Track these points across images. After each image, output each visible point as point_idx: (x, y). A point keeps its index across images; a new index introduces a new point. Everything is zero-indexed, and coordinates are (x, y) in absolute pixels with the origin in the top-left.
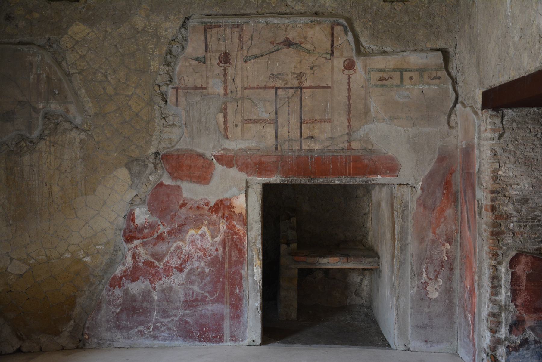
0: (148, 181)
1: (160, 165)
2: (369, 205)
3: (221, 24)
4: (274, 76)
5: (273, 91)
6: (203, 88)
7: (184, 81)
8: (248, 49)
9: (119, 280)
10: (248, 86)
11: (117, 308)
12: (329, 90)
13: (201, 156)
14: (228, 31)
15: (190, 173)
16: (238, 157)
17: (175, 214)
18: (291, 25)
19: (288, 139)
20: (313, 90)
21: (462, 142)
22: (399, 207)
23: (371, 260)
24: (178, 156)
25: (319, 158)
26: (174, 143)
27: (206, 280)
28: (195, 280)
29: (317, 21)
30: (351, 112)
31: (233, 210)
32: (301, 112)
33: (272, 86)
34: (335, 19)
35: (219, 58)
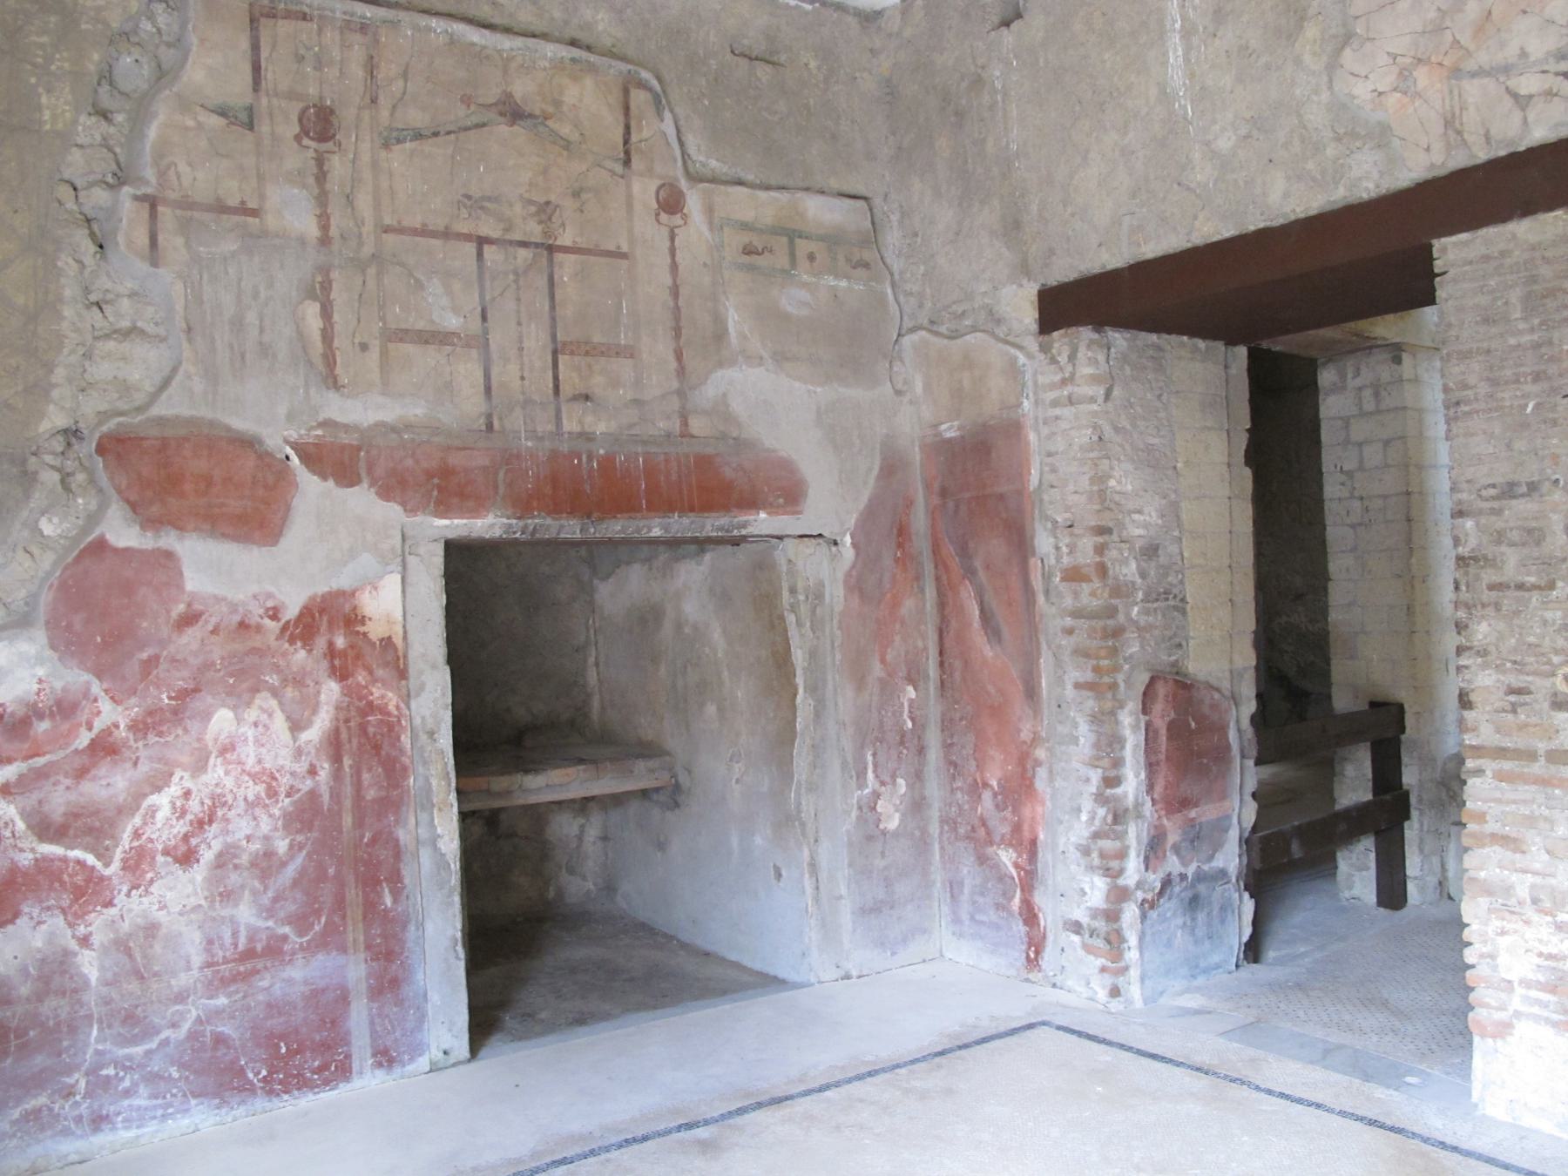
1: (81, 477)
4: (473, 203)
5: (471, 248)
7: (179, 178)
8: (394, 107)
10: (395, 223)
12: (624, 263)
13: (248, 443)
14: (330, 36)
18: (519, 59)
19: (521, 398)
21: (936, 426)
22: (802, 598)
23: (652, 764)
24: (164, 444)
26: (139, 398)
27: (280, 881)
28: (243, 887)
29: (588, 62)
30: (684, 331)
32: (553, 319)
33: (465, 231)
34: (630, 67)
35: (300, 120)
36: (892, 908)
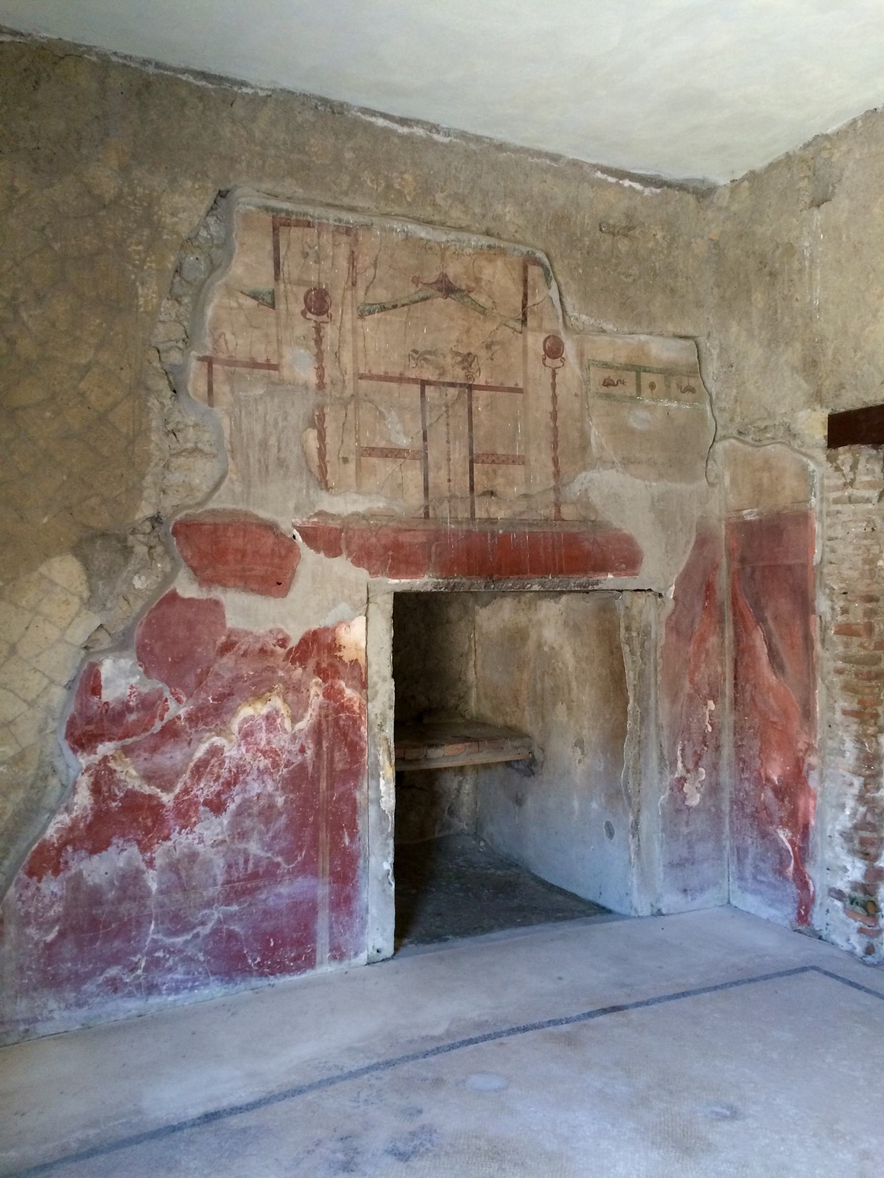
0: (133, 591)
1: (160, 549)
2: (469, 637)
3: (310, 219)
4: (419, 356)
5: (416, 388)
6: (269, 366)
8: (368, 288)
9: (53, 853)
11: (48, 931)
12: (520, 396)
13: (270, 527)
14: (326, 238)
15: (244, 570)
16: (351, 533)
17: (208, 672)
18: (452, 248)
19: (448, 494)
20: (493, 393)
25: (506, 536)
26: (200, 496)
27: (277, 826)
28: (253, 829)
29: (499, 247)
31: (339, 654)
32: (471, 438)
33: (413, 377)
36: (693, 864)
